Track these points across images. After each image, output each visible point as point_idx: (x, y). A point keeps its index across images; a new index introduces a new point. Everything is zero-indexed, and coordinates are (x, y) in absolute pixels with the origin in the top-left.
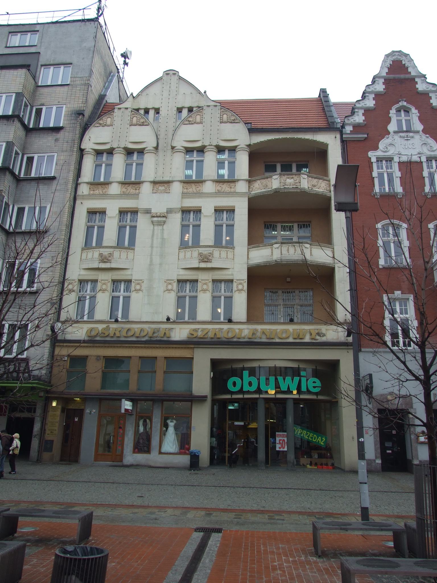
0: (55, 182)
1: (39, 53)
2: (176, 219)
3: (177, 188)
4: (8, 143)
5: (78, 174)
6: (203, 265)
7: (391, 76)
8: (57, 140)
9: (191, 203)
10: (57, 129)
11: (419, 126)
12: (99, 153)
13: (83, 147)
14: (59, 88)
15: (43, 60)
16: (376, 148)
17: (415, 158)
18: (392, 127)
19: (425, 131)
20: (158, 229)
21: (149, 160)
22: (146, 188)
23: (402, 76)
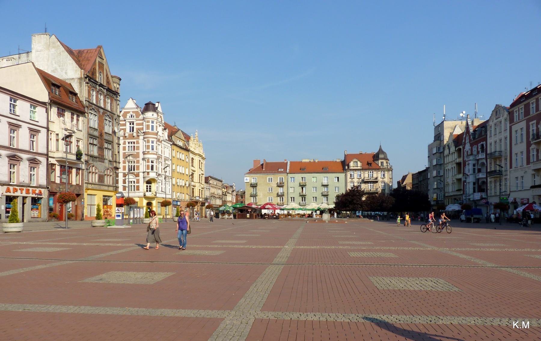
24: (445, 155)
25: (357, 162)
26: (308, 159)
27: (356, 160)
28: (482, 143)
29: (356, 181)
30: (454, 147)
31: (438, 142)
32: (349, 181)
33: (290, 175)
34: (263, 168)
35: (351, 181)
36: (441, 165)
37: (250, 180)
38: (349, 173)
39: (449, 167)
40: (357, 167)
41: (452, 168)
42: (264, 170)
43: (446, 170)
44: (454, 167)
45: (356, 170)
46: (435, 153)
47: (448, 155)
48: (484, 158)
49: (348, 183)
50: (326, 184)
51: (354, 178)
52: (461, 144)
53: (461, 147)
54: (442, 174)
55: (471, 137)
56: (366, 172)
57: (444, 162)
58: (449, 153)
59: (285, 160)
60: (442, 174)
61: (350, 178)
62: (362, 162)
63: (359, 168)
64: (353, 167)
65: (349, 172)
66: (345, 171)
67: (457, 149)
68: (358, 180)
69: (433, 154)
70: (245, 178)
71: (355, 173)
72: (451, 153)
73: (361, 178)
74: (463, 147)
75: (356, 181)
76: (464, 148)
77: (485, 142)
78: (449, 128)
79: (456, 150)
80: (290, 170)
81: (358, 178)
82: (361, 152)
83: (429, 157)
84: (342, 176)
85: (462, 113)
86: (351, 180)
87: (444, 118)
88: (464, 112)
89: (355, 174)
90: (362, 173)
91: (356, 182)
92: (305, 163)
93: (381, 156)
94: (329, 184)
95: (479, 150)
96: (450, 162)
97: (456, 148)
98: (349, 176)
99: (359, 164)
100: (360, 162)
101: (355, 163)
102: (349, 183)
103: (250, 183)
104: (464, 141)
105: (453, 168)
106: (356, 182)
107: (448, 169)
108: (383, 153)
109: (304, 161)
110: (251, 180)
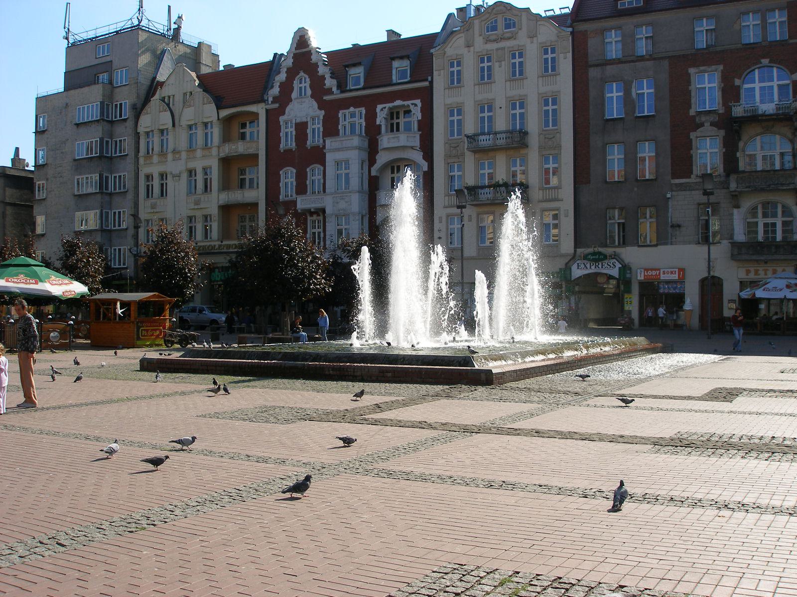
0: (128, 157)
2: (185, 176)
3: (184, 155)
5: (138, 151)
6: (196, 207)
7: (297, 51)
8: (126, 127)
9: (191, 165)
10: (125, 120)
11: (309, 92)
12: (147, 133)
13: (138, 131)
14: (123, 87)
15: (114, 67)
16: (284, 113)
17: (304, 120)
18: (294, 95)
19: (312, 96)
20: (177, 183)
21: (171, 137)
22: (170, 157)
23: (304, 50)
24: (141, 130)
28: (398, 103)
43: (149, 177)
46: (98, 121)
48: (412, 148)
52: (262, 100)
53: (260, 109)
55: (330, 83)
58: (174, 125)
67: (225, 113)
69: (78, 125)
74: (267, 111)
77: (418, 102)
79: (221, 117)
83: (37, 133)
95: (378, 123)
97: (219, 108)
104: (275, 91)
107: (163, 176)
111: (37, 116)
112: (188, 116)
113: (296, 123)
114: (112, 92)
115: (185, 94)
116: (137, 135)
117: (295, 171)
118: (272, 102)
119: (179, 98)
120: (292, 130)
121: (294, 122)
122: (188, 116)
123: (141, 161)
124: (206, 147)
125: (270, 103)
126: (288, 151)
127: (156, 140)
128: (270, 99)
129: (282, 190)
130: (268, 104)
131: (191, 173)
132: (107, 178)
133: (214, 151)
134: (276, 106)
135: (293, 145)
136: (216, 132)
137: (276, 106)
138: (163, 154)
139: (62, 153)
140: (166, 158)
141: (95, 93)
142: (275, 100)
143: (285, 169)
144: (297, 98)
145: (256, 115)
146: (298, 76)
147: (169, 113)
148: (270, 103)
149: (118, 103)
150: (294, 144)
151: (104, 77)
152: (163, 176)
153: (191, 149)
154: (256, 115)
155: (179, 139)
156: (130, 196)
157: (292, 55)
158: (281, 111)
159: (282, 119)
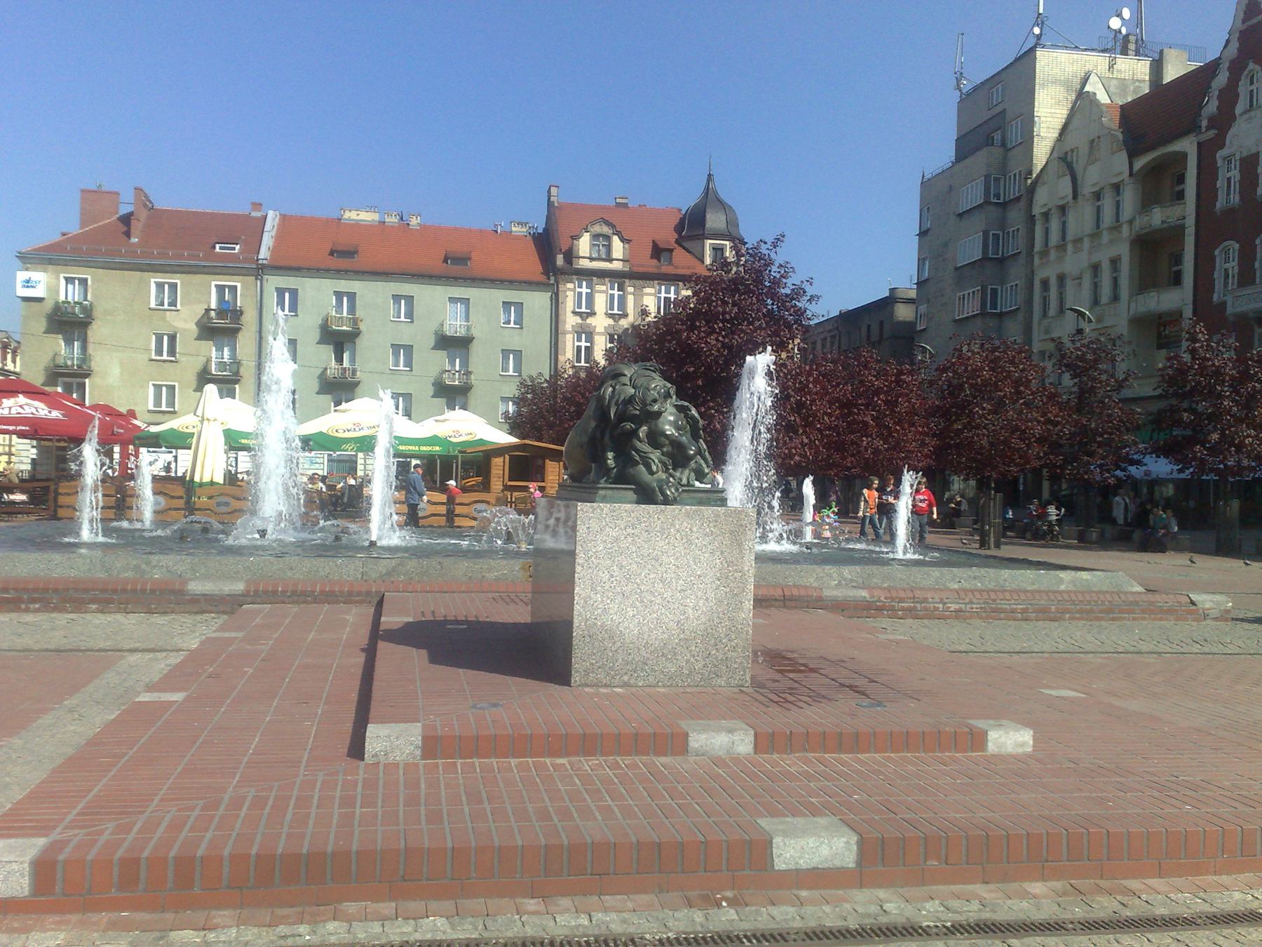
1: (1005, 110)
3: (1086, 243)
4: (983, 231)
9: (1095, 259)
16: (1222, 146)
18: (1239, 110)
22: (1070, 247)
24: (1037, 210)
25: (608, 238)
26: (371, 208)
27: (606, 230)
29: (600, 329)
30: (1123, 156)
31: (981, 161)
32: (568, 327)
33: (273, 282)
34: (128, 234)
35: (581, 326)
36: (1001, 261)
37: (49, 289)
38: (570, 286)
39: (1074, 263)
40: (610, 260)
41: (1096, 268)
42: (134, 240)
43: (1045, 284)
44: (1115, 262)
45: (602, 274)
46: (980, 206)
47: (1063, 209)
49: (565, 333)
50: (461, 332)
51: (593, 314)
52: (1192, 128)
53: (1188, 146)
54: (1005, 305)
56: (648, 290)
57: (1033, 246)
58: (1075, 196)
59: (257, 206)
60: (1005, 305)
61: (574, 313)
62: (629, 241)
63: (617, 266)
64: (591, 259)
65: (571, 282)
66: (552, 278)
67: (1139, 163)
68: (611, 322)
69: (960, 215)
70: (22, 276)
71: (598, 287)
72: (1087, 189)
73: (625, 316)
75: (600, 329)
76: (1207, 152)
78: (1055, 82)
80: (275, 250)
81: (612, 316)
82: (624, 201)
83: (923, 234)
84: (537, 302)
85: (1119, 15)
86: (578, 320)
87: (1037, 31)
88: (1126, 13)
89: (597, 295)
90: (631, 289)
91: (599, 334)
92: (357, 225)
93: (714, 220)
94: (475, 332)
96: (1078, 241)
97: (1132, 155)
98: (569, 303)
99: (618, 248)
100: (622, 240)
101: (602, 242)
102: (569, 337)
103: (48, 306)
105: (1106, 266)
106: (599, 334)
107: (1061, 279)
108: (723, 206)
109: (351, 215)
110: (54, 290)
111: (921, 210)
112: (1092, 177)
113: (1241, 159)
114: (1005, 157)
115: (1092, 141)
116: (1031, 219)
117: (1237, 246)
118: (1208, 128)
119: (1084, 150)
120: (1235, 174)
121: (1238, 157)
122: (1092, 177)
123: (1037, 260)
124: (1116, 228)
125: (1204, 130)
126: (1230, 212)
127: (1055, 225)
128: (1204, 123)
129: (1218, 285)
130: (1200, 133)
131: (1096, 268)
132: (994, 292)
133: (1125, 230)
134: (1212, 133)
135: (1235, 199)
136: (1129, 198)
137: (1212, 133)
138: (1062, 247)
139: (944, 260)
140: (1065, 250)
141: (981, 161)
142: (1213, 123)
143: (1226, 243)
144: (1245, 112)
145: (1183, 156)
146: (1246, 73)
147: (1068, 178)
148: (1204, 130)
149: (1012, 174)
150: (1237, 198)
151: (997, 137)
152: (1061, 279)
153: (1095, 235)
154: (1183, 156)
155: (1080, 220)
156: (1021, 316)
157: (1237, 35)
158: (1219, 142)
159: (1220, 154)
